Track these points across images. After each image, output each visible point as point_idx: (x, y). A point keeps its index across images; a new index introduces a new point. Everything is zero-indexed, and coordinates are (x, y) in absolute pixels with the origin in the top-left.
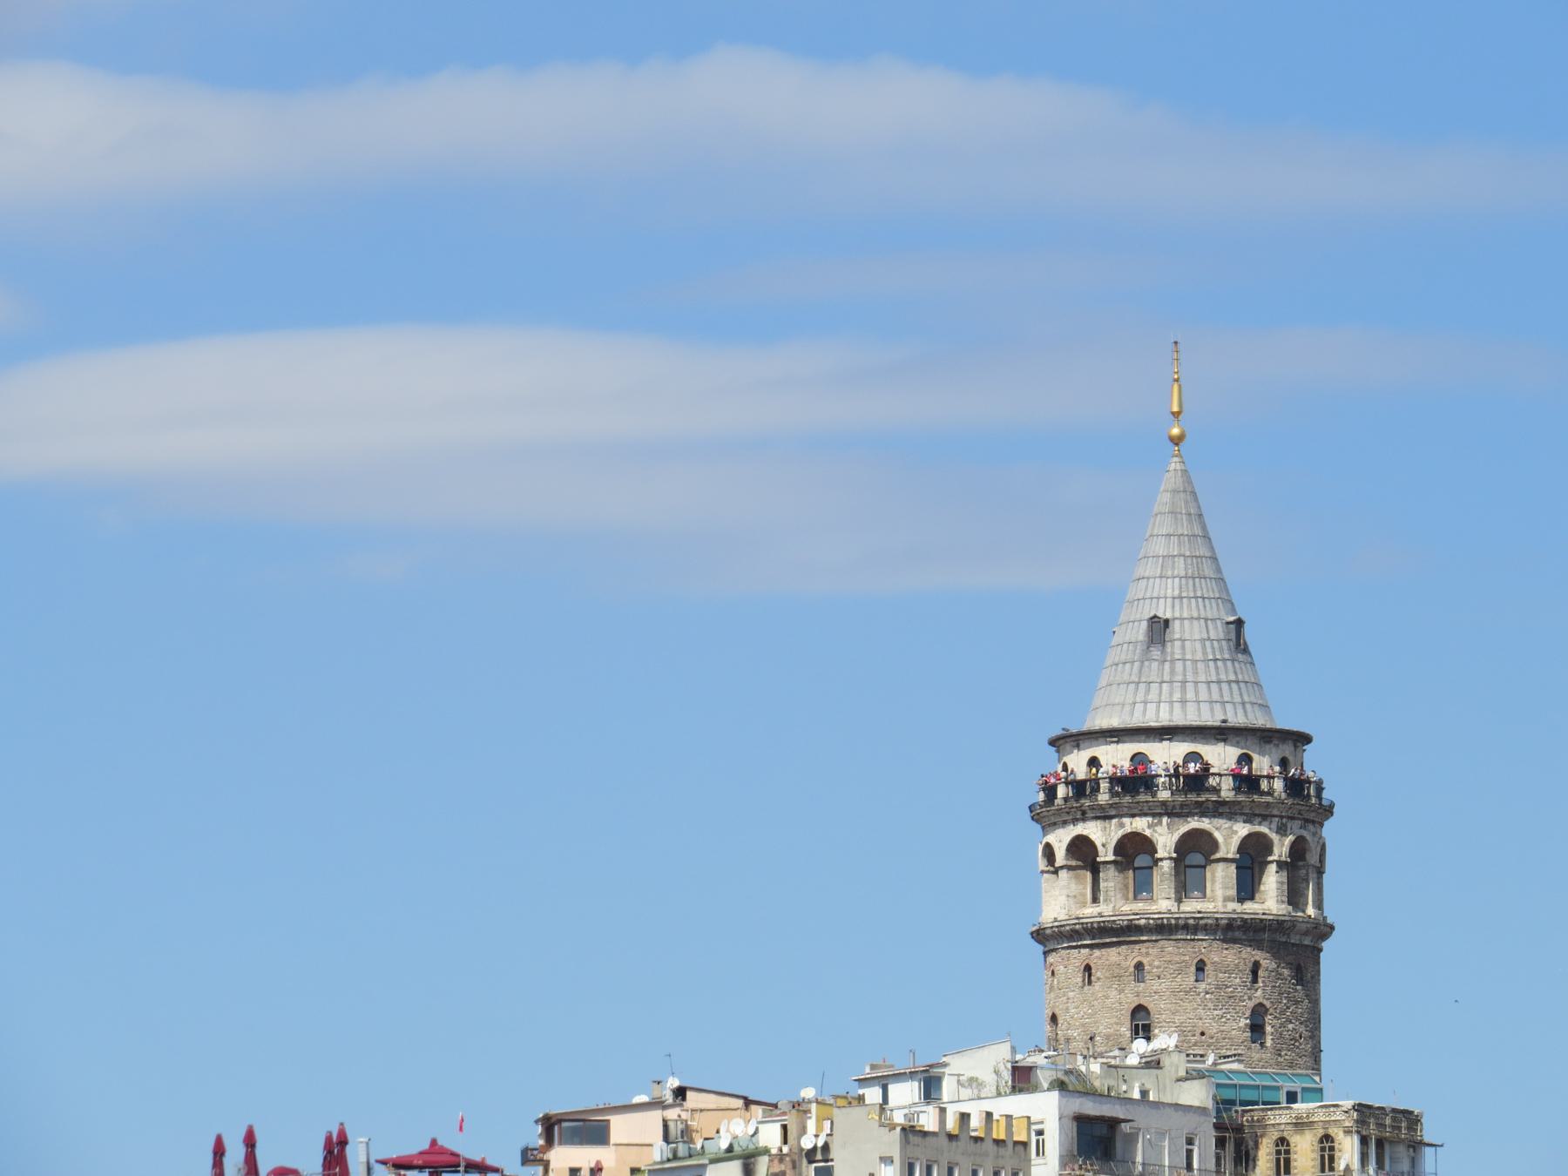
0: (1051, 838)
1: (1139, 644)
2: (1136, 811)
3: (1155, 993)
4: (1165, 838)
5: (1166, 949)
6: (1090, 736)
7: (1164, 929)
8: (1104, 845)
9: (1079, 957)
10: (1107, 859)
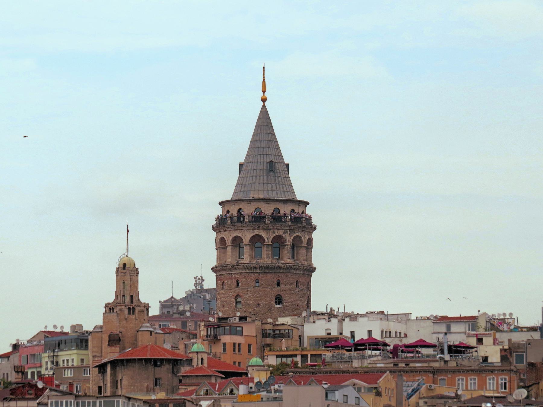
0: (222, 235)
1: (265, 170)
2: (279, 228)
3: (284, 290)
4: (289, 239)
5: (288, 276)
6: (258, 201)
7: (289, 268)
8: (267, 238)
9: (253, 277)
10: (269, 244)
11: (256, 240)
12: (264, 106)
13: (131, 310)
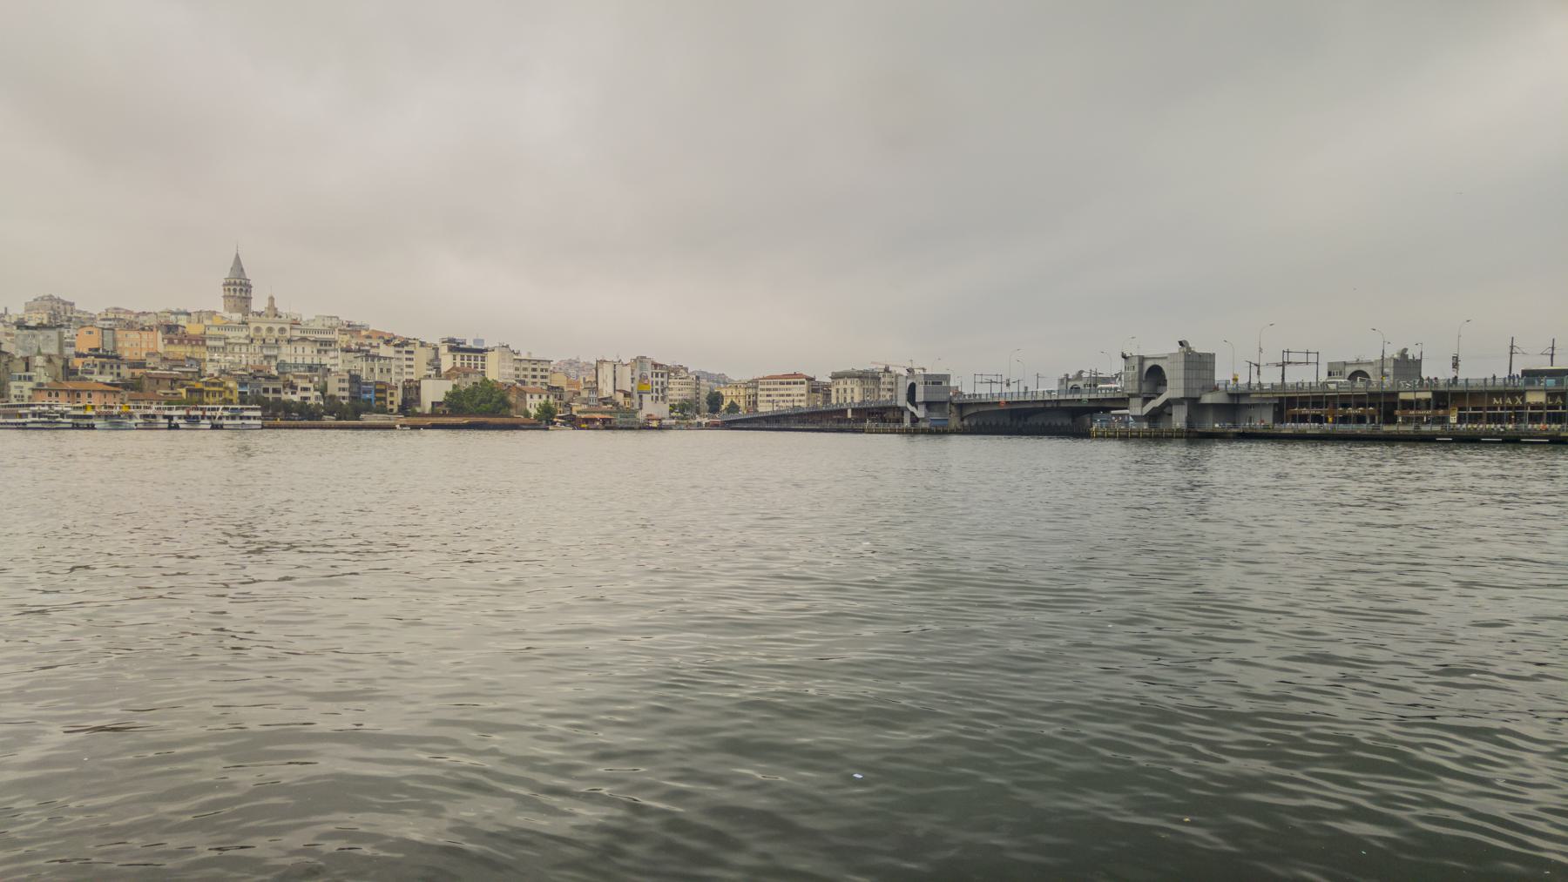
11: (241, 290)
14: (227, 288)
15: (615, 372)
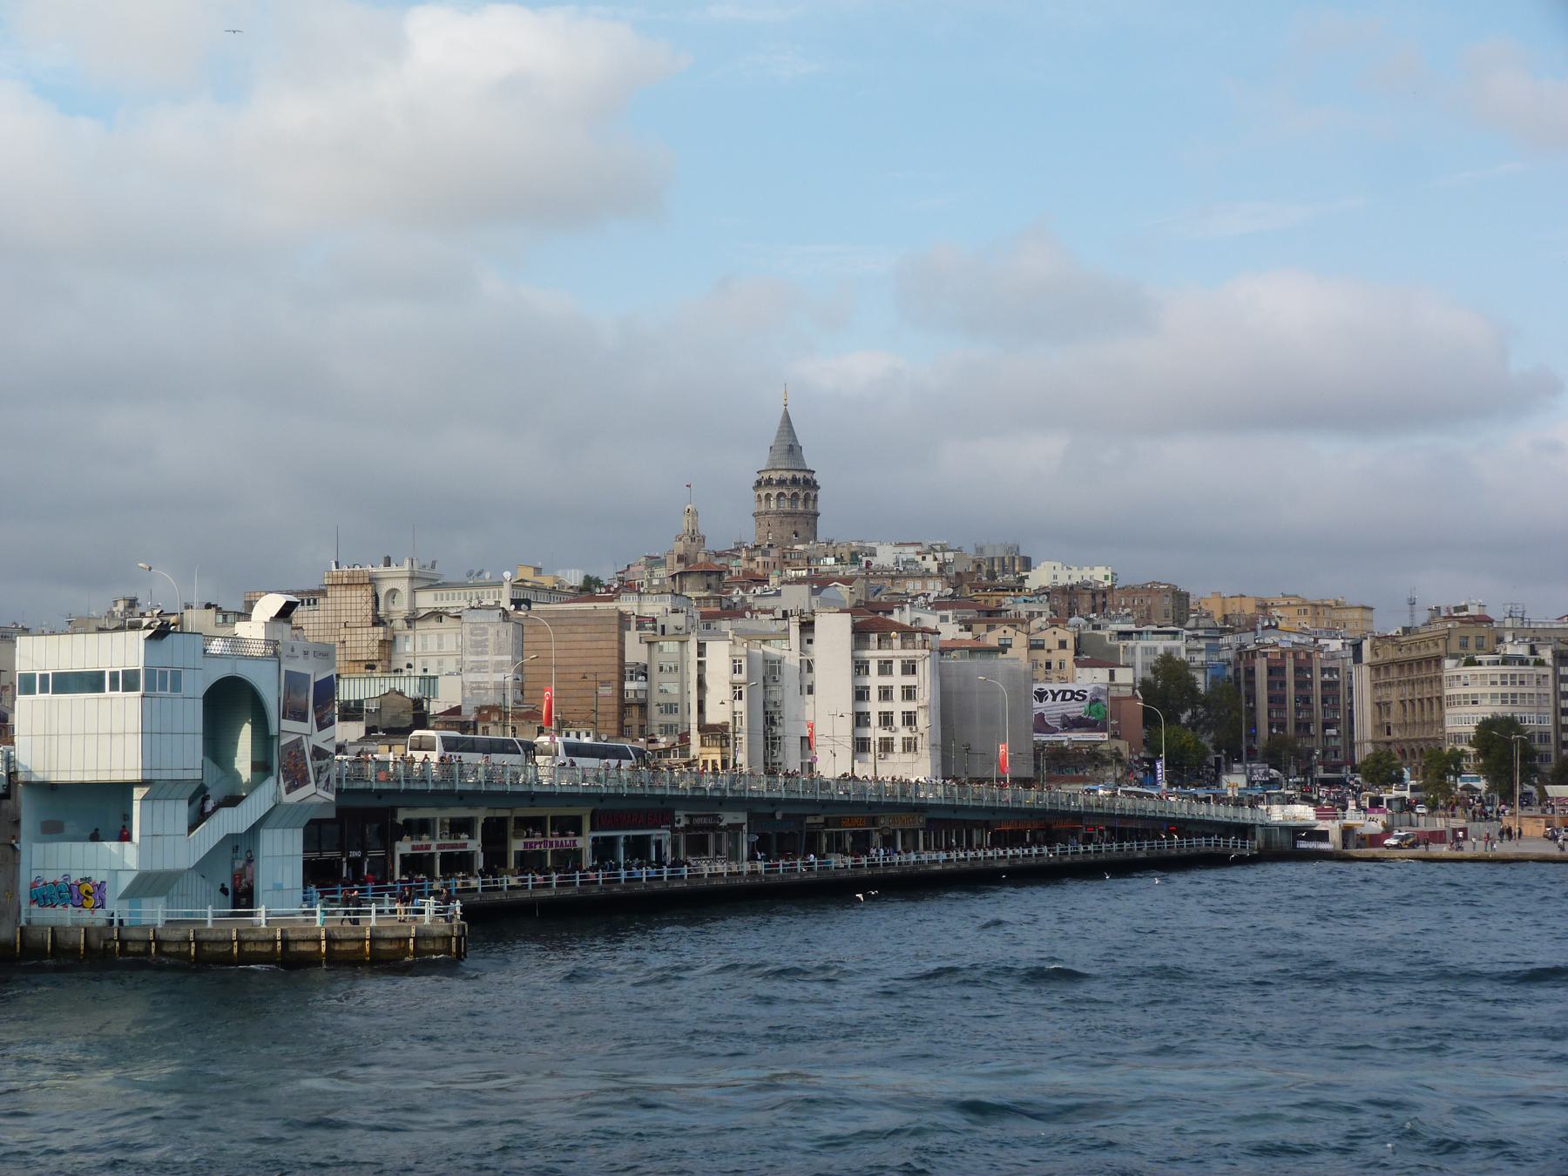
0: (759, 492)
4: (802, 495)
11: (780, 495)
12: (786, 410)
13: (693, 540)
14: (763, 493)
15: (701, 664)
